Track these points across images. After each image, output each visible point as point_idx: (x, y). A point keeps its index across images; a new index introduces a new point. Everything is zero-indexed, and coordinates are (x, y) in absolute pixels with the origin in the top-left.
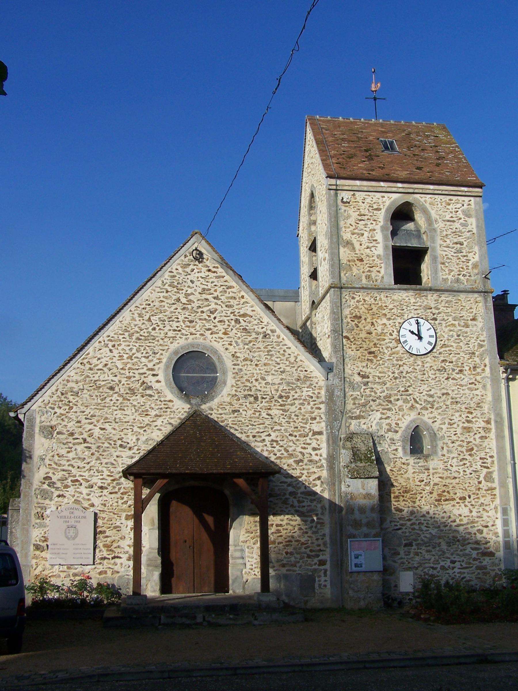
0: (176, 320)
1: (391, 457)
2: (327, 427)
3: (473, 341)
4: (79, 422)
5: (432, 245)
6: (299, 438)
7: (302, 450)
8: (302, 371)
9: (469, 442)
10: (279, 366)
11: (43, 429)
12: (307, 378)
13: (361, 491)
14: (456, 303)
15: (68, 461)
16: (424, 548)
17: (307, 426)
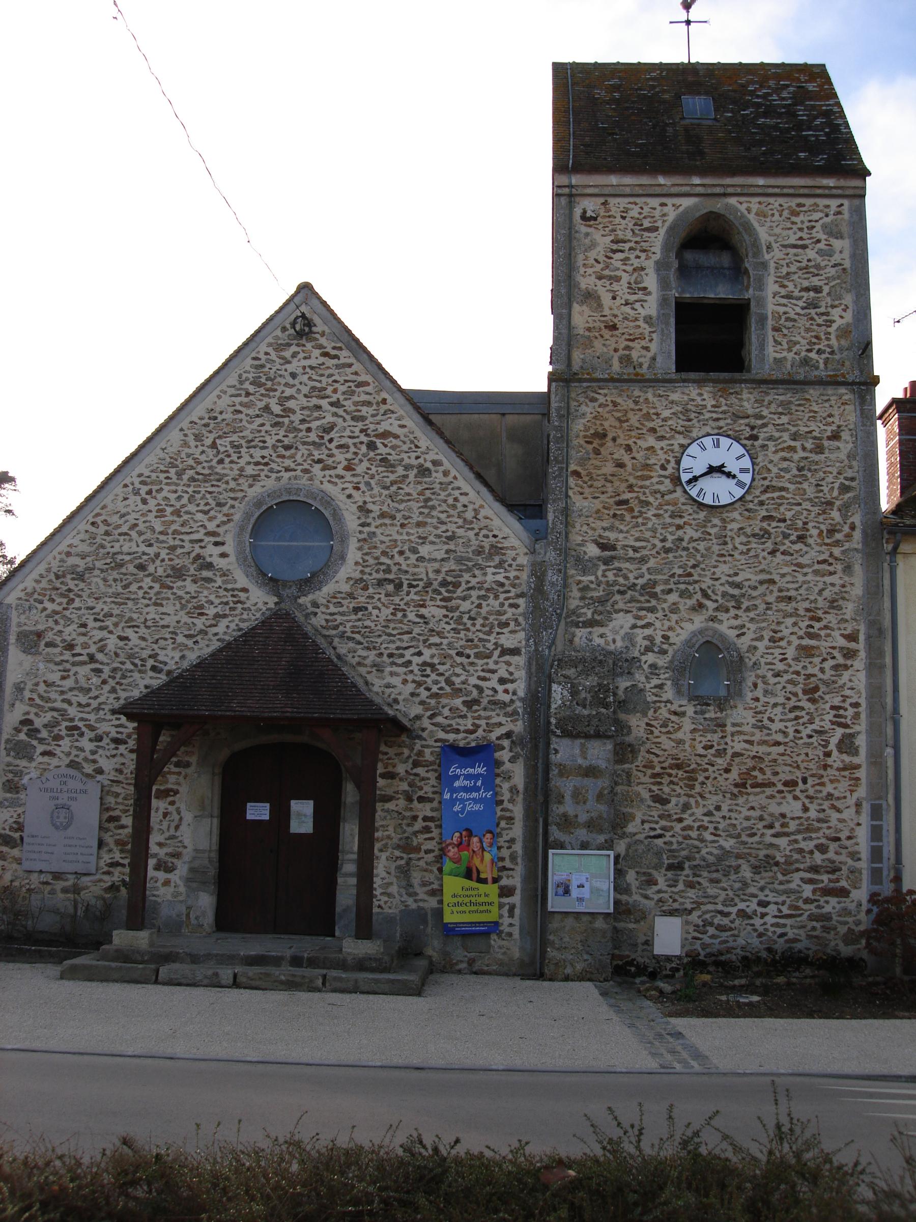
0: (261, 444)
1: (649, 699)
2: (528, 640)
3: (830, 479)
4: (84, 625)
5: (757, 293)
6: (476, 661)
7: (480, 683)
8: (487, 536)
9: (809, 676)
10: (444, 528)
11: (22, 636)
12: (496, 550)
13: (580, 761)
14: (799, 405)
15: (62, 693)
16: (705, 874)
17: (492, 638)
